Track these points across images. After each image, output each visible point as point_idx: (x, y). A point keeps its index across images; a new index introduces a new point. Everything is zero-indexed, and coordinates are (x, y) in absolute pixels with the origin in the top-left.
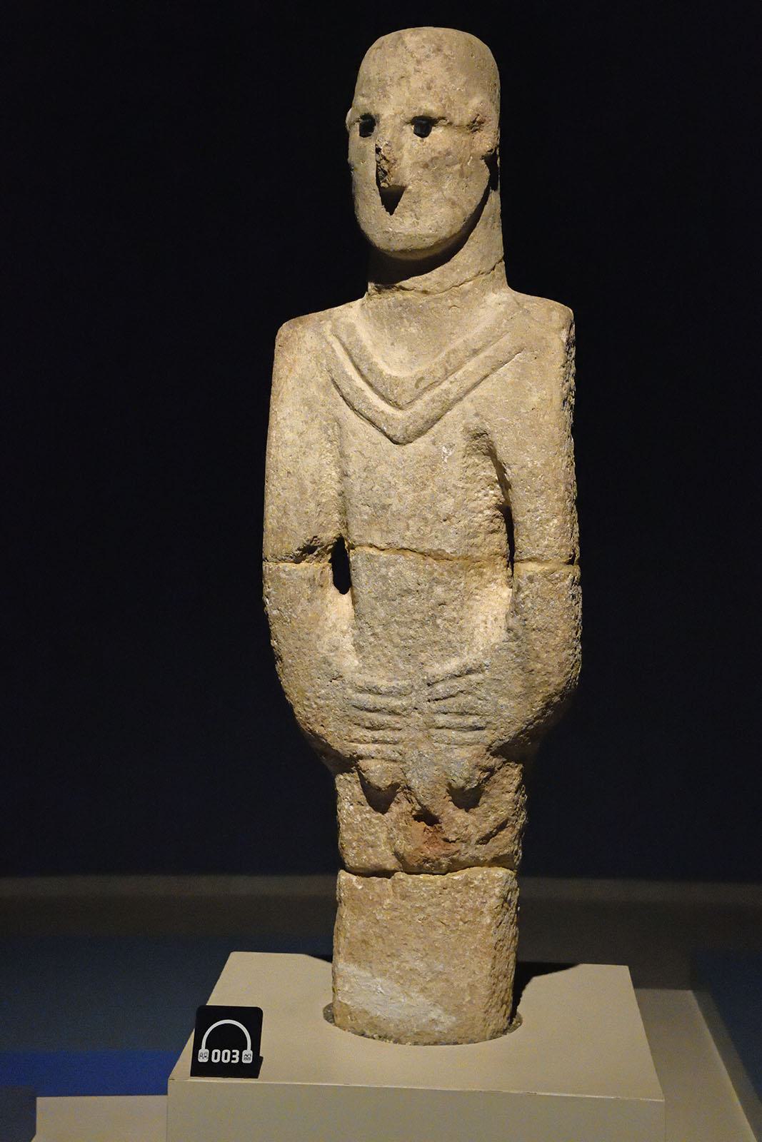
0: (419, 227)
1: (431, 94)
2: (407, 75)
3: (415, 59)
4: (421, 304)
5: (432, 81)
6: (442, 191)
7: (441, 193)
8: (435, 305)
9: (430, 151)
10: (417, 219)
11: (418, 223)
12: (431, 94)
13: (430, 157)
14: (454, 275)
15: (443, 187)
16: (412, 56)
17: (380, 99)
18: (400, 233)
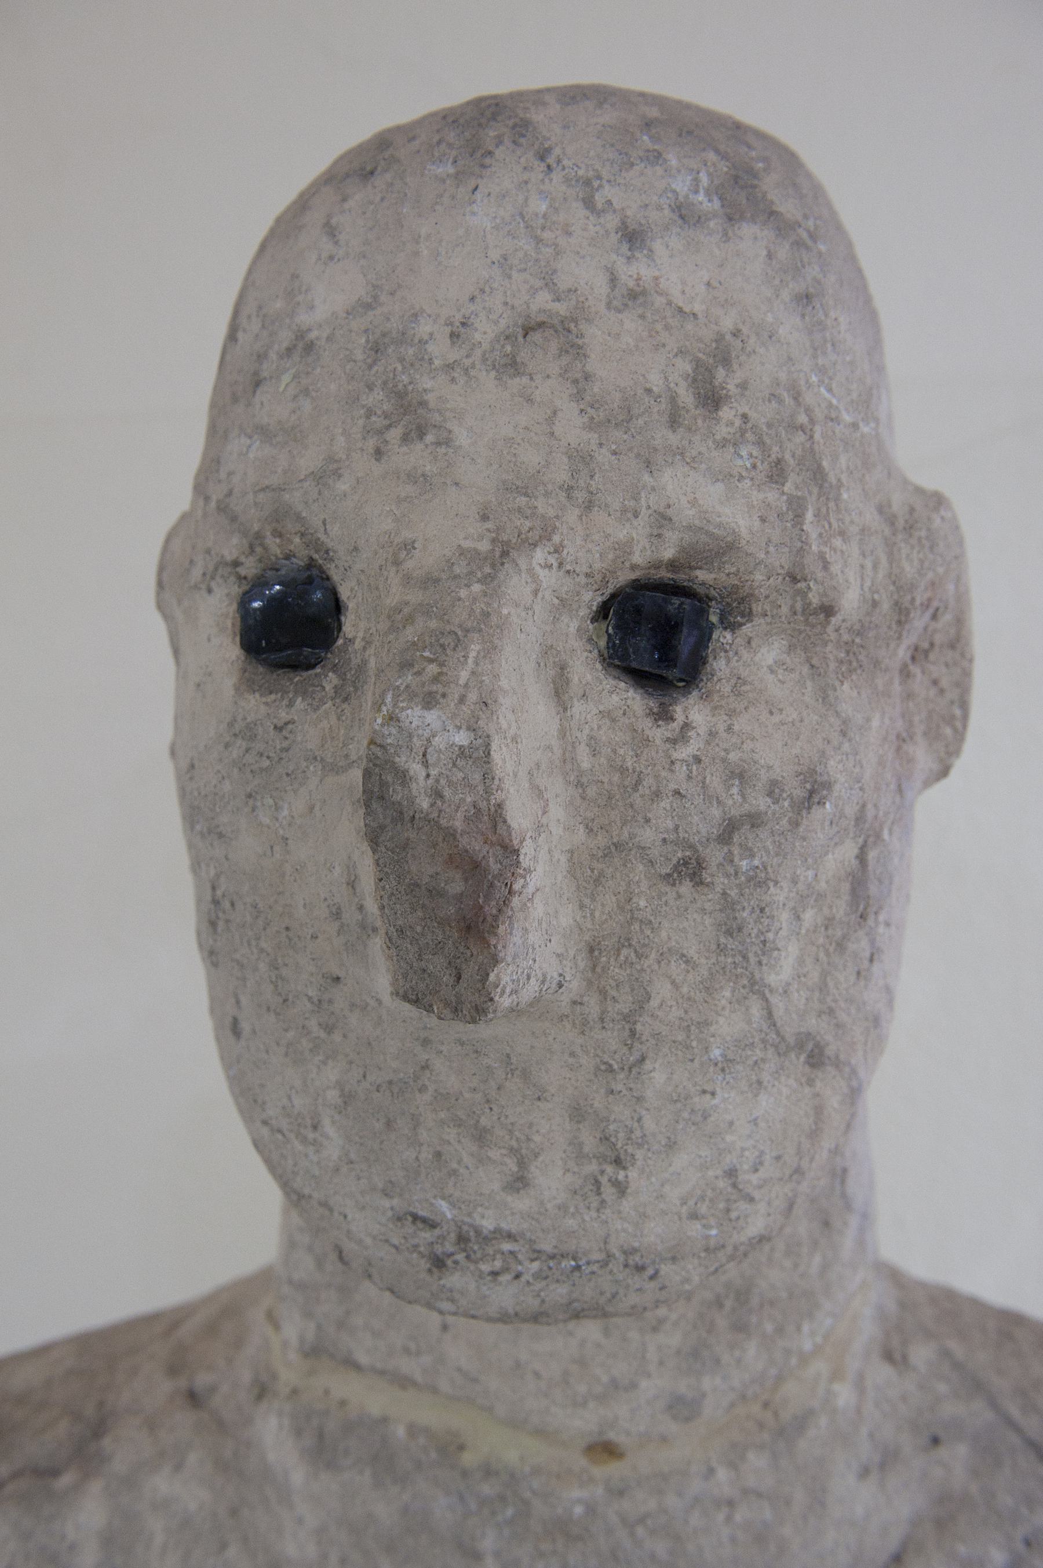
0: (627, 1205)
1: (722, 431)
2: (562, 308)
3: (611, 221)
4: (579, 1501)
5: (726, 361)
6: (757, 987)
7: (756, 1010)
8: (652, 1504)
9: (715, 782)
10: (618, 1162)
11: (621, 1189)
12: (722, 431)
13: (716, 812)
14: (752, 1349)
15: (772, 979)
16: (589, 203)
17: (378, 453)
18: (510, 1236)
